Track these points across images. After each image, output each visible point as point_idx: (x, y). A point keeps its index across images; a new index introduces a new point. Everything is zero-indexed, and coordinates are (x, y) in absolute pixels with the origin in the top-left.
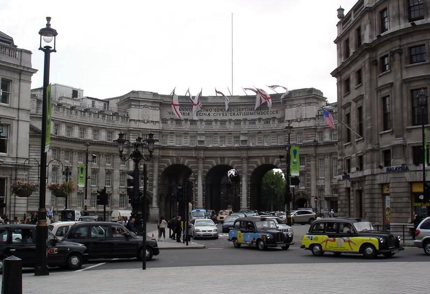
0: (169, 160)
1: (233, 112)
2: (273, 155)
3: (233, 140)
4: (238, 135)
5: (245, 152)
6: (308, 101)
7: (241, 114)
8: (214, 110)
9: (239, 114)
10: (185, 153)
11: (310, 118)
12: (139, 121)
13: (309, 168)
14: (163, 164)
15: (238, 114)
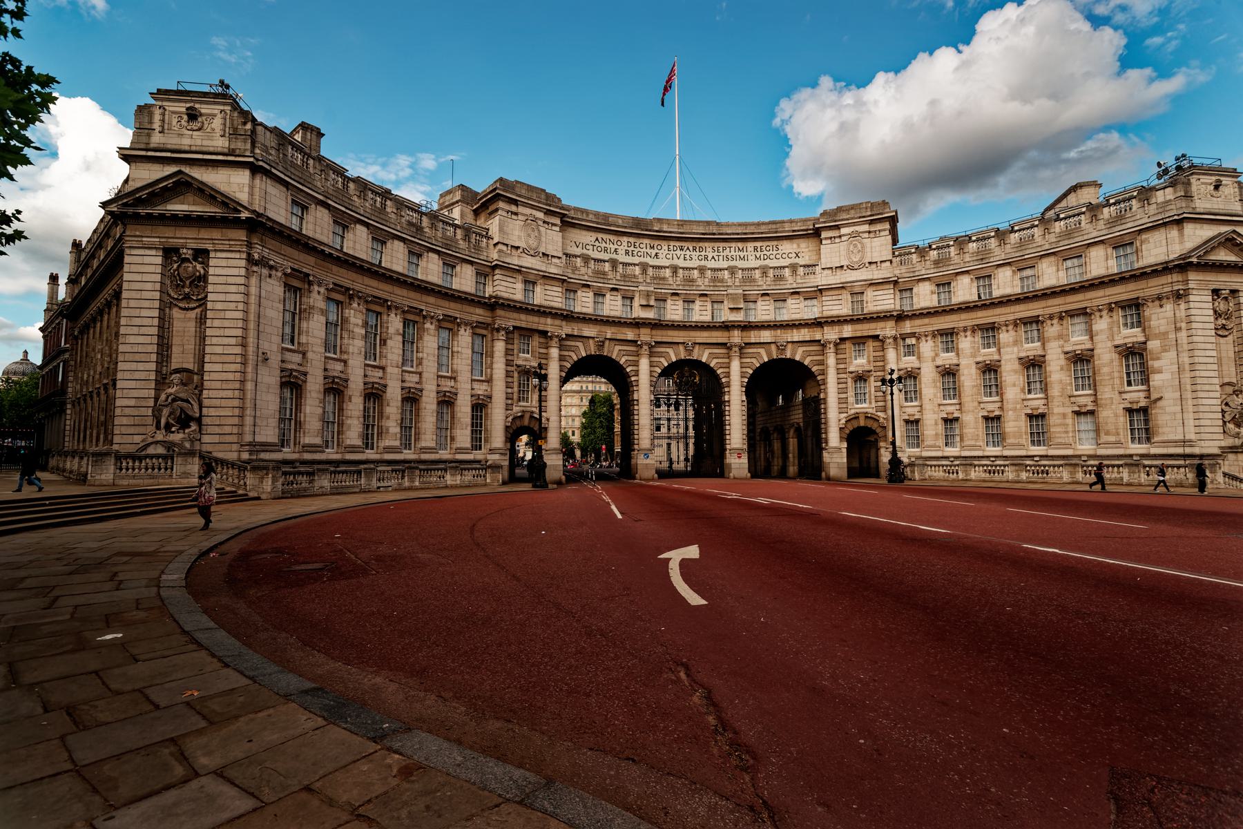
0: (580, 344)
1: (703, 253)
2: (795, 340)
3: (709, 307)
4: (720, 299)
5: (736, 333)
6: (873, 228)
7: (721, 258)
8: (666, 248)
9: (716, 258)
10: (609, 332)
11: (881, 262)
12: (517, 248)
13: (881, 364)
14: (566, 353)
15: (713, 258)
